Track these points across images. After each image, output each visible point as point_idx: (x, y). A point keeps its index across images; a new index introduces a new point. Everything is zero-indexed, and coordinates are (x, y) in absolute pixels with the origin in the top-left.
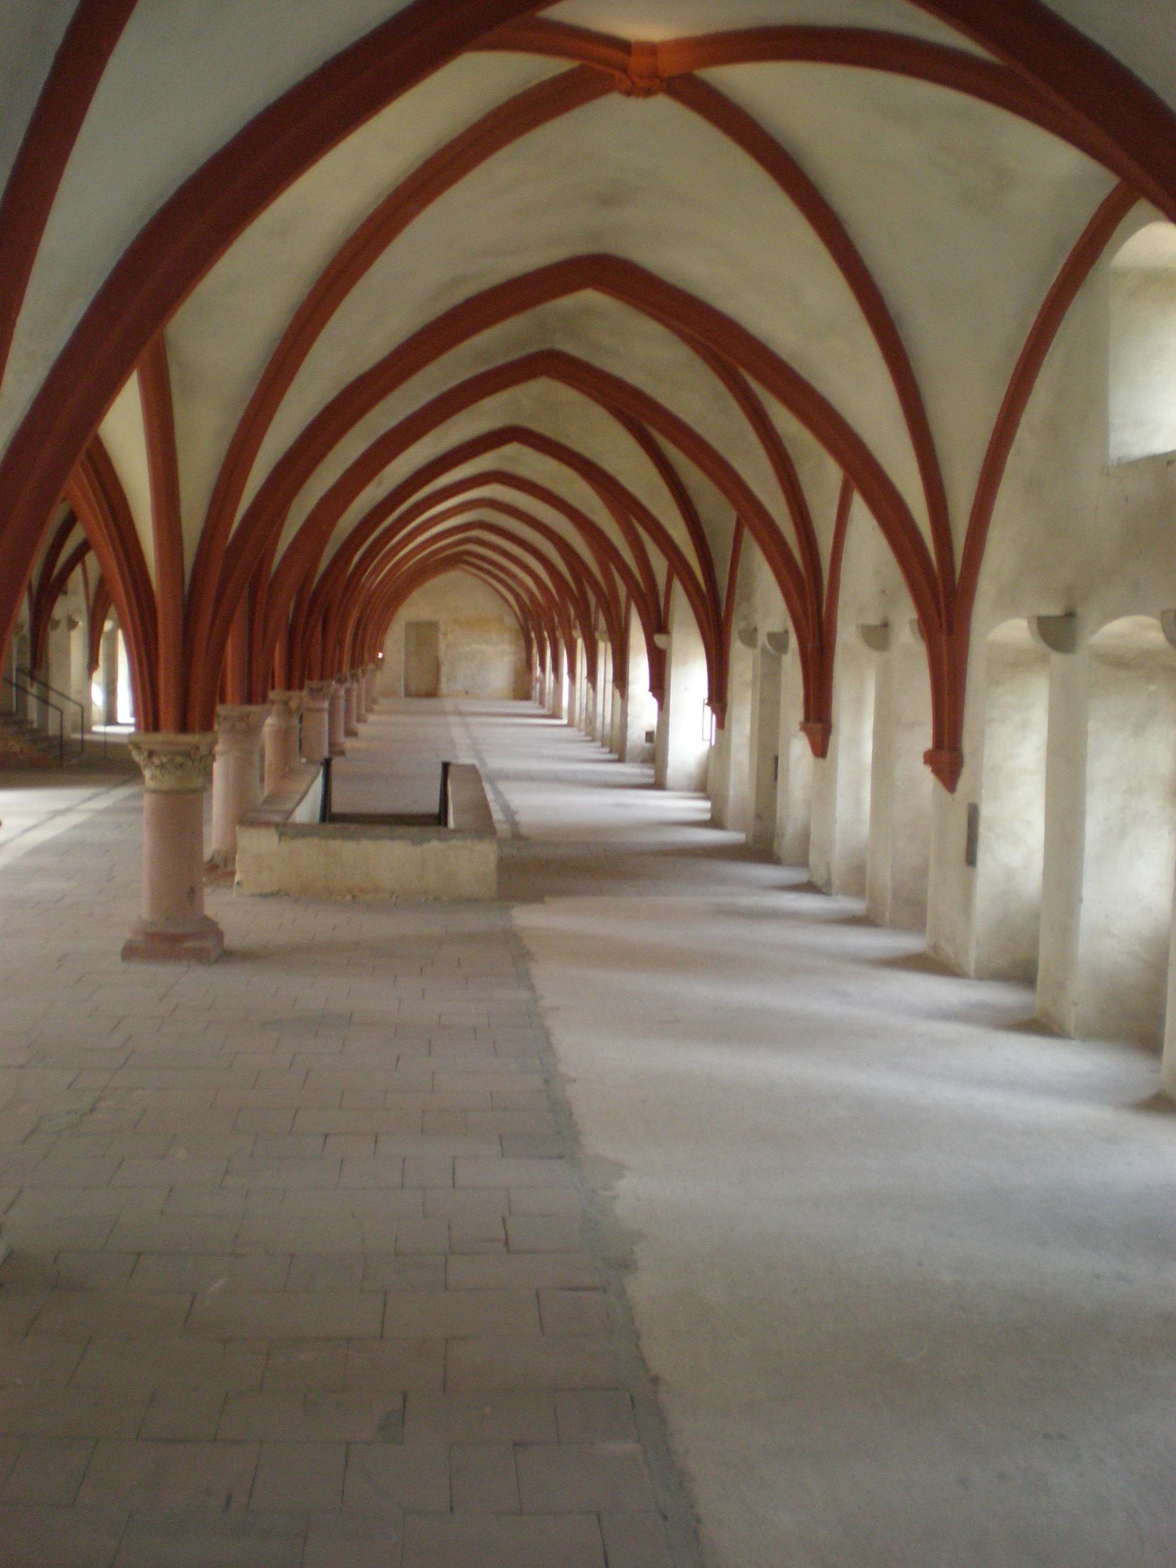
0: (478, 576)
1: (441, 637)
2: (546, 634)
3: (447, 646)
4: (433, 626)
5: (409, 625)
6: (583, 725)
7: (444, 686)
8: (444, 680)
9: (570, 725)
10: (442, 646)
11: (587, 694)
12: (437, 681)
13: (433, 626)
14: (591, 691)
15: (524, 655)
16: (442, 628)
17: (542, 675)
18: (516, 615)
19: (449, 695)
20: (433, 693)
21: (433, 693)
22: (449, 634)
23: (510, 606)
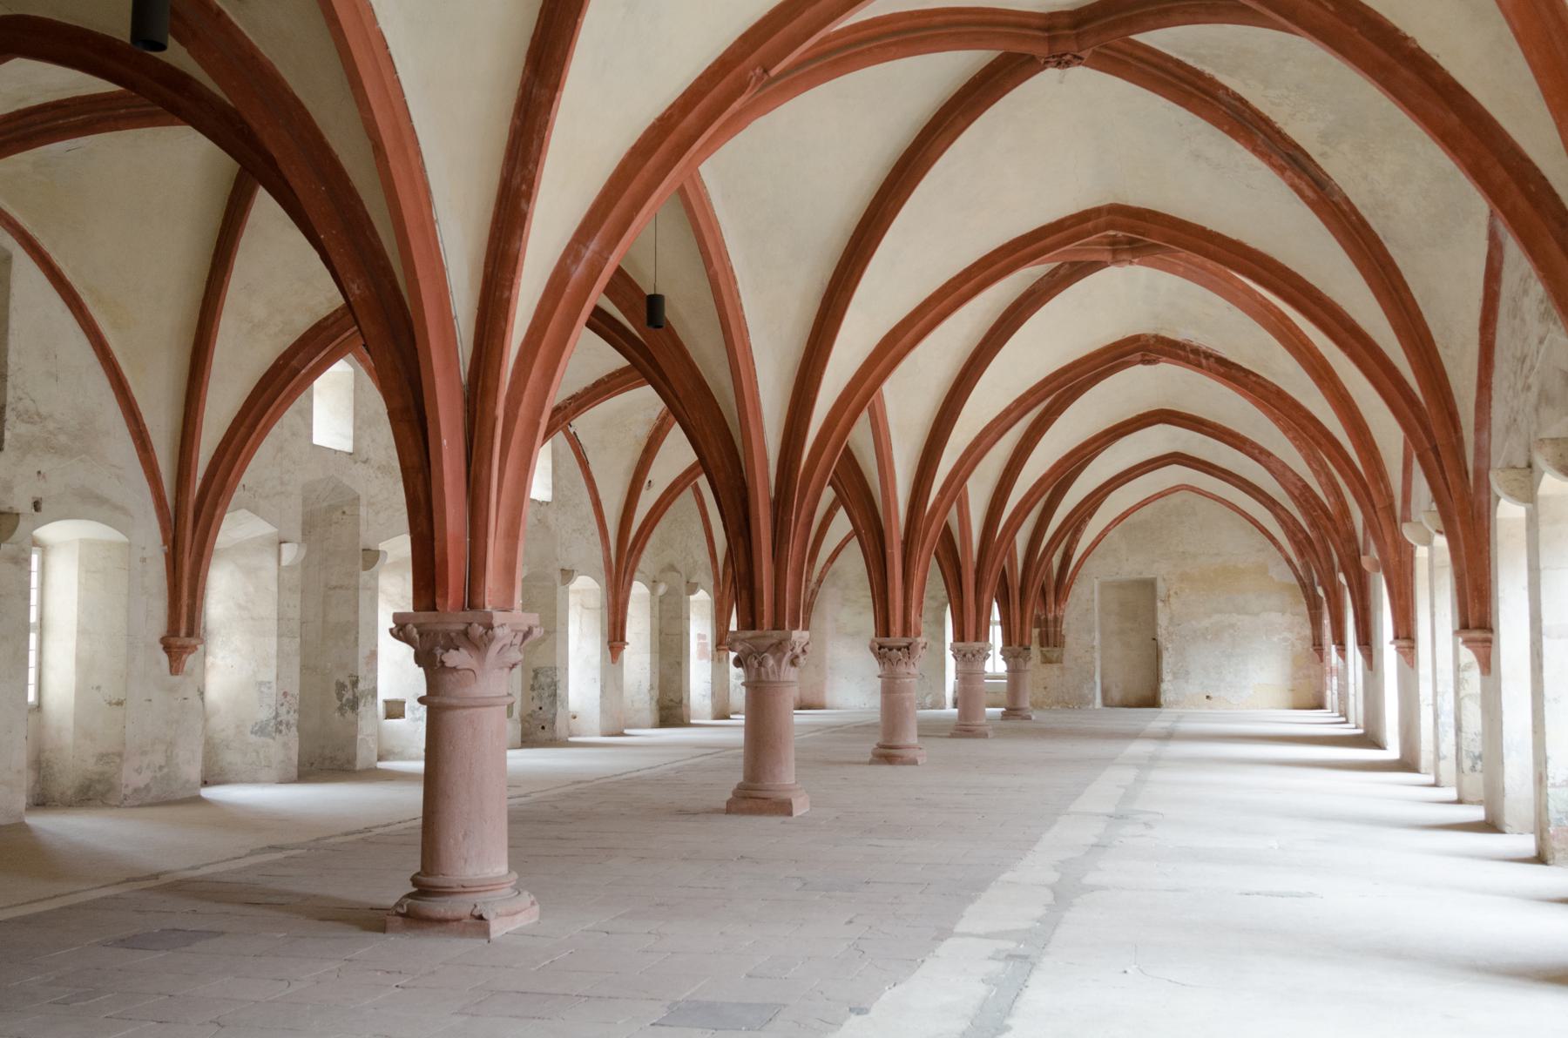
0: (940, 134)
1: (1160, 604)
2: (1342, 578)
3: (1171, 619)
4: (1149, 586)
5: (1105, 586)
6: (1448, 768)
7: (1168, 688)
8: (1167, 676)
9: (1407, 764)
10: (1163, 619)
11: (1458, 683)
12: (1157, 678)
13: (1149, 586)
14: (1474, 676)
15: (1307, 631)
16: (1161, 588)
17: (1340, 660)
18: (1289, 561)
19: (1177, 703)
20: (1151, 700)
21: (1151, 700)
22: (1171, 599)
23: (1280, 548)
